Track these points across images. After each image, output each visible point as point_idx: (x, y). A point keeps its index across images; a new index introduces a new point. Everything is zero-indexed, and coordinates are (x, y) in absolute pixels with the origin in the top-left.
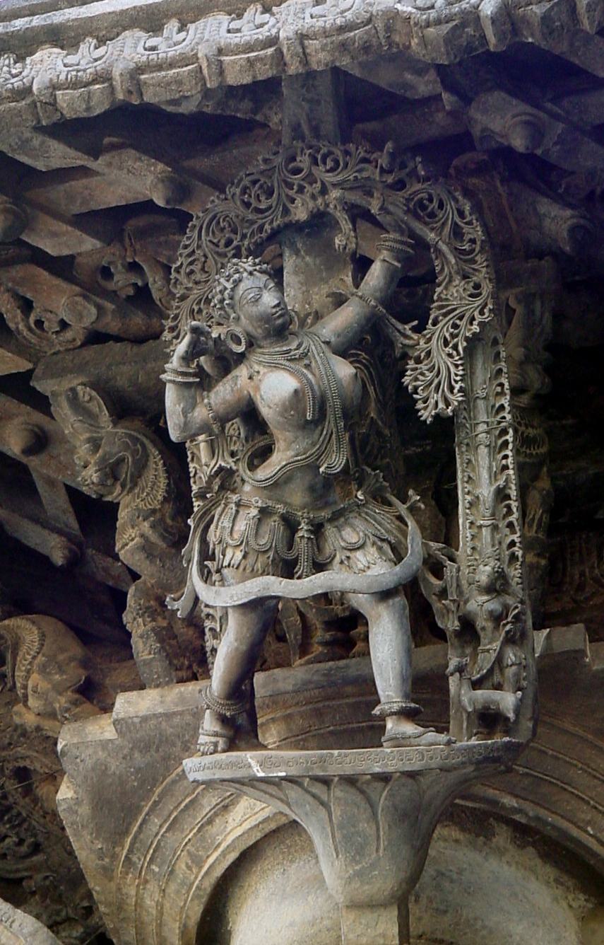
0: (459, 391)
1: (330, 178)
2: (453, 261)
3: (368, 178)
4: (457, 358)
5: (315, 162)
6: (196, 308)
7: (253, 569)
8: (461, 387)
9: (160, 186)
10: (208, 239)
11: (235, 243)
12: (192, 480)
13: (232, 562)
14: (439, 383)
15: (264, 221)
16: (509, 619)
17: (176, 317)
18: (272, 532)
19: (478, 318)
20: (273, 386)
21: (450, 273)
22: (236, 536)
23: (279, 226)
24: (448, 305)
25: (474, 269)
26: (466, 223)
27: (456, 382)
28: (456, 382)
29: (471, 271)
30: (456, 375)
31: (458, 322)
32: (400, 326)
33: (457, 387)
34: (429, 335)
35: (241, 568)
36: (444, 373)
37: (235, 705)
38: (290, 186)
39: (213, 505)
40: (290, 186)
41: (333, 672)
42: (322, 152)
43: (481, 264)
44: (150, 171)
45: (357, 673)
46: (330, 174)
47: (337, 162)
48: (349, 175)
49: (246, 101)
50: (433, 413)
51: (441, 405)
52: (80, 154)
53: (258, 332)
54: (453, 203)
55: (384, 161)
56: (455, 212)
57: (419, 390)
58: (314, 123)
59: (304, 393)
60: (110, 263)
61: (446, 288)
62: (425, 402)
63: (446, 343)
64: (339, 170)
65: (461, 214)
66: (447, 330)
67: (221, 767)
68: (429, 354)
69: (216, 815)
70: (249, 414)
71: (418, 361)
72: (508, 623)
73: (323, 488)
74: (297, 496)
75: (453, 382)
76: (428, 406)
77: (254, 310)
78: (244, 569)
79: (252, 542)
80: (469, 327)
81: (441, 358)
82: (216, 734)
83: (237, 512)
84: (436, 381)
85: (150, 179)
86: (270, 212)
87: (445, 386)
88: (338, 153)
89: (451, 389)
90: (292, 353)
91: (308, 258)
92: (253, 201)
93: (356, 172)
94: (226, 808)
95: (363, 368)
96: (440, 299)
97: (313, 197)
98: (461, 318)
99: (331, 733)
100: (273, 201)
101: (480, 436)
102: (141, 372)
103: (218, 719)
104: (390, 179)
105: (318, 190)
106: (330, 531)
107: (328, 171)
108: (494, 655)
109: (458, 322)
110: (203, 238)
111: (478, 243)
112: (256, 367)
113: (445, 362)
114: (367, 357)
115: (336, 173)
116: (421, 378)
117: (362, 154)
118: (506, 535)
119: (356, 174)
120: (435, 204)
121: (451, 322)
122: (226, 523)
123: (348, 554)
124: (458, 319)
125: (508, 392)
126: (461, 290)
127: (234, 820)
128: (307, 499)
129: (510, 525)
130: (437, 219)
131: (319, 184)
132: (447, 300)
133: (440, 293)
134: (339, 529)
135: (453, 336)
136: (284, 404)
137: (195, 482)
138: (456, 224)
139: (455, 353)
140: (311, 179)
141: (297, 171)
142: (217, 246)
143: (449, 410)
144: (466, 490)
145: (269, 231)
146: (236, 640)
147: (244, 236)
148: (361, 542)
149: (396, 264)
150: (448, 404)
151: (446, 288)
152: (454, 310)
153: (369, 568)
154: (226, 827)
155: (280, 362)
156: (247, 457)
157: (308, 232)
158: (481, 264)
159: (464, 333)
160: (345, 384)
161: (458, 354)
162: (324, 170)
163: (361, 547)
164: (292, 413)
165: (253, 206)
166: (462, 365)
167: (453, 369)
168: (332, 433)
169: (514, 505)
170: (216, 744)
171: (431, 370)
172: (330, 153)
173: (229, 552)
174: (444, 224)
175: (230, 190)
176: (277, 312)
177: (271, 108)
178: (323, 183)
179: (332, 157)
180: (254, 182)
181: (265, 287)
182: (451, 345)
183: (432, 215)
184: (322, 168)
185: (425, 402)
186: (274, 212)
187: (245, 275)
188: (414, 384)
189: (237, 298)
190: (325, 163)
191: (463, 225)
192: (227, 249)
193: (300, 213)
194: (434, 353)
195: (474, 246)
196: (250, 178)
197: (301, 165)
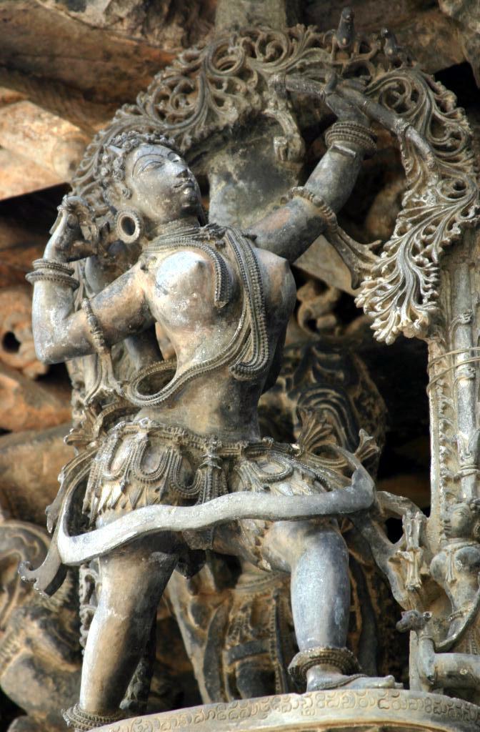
0: (429, 300)
1: (267, 69)
4: (430, 265)
9: (64, 147)
14: (404, 294)
15: (183, 130)
18: (166, 459)
21: (424, 173)
22: (116, 466)
23: (202, 135)
24: (420, 211)
28: (426, 290)
30: (427, 283)
31: (433, 228)
32: (356, 245)
33: (427, 295)
40: (219, 85)
43: (465, 161)
44: (52, 134)
46: (271, 64)
47: (279, 50)
48: (295, 61)
49: (174, 25)
50: (394, 329)
55: (338, 39)
57: (377, 308)
60: (14, 326)
64: (282, 57)
66: (417, 238)
75: (422, 292)
76: (388, 323)
84: (400, 293)
85: (52, 143)
86: (191, 119)
89: (420, 300)
91: (241, 184)
95: (332, 408)
97: (247, 94)
101: (460, 368)
102: (46, 458)
105: (254, 85)
107: (268, 61)
109: (433, 228)
111: (464, 138)
114: (338, 395)
117: (312, 35)
120: (408, 94)
123: (267, 485)
124: (433, 224)
126: (438, 191)
128: (217, 426)
130: (408, 113)
131: (255, 78)
133: (410, 197)
135: (425, 244)
136: (183, 284)
140: (244, 74)
143: (415, 324)
145: (189, 142)
149: (350, 151)
151: (419, 192)
156: (138, 381)
157: (243, 153)
158: (465, 161)
161: (431, 260)
162: (262, 59)
166: (434, 272)
167: (422, 278)
173: (106, 490)
175: (140, 99)
178: (261, 78)
180: (172, 87)
182: (422, 253)
185: (382, 320)
186: (195, 119)
190: (264, 53)
191: (443, 118)
193: (229, 115)
194: (400, 266)
195: (457, 141)
197: (232, 58)
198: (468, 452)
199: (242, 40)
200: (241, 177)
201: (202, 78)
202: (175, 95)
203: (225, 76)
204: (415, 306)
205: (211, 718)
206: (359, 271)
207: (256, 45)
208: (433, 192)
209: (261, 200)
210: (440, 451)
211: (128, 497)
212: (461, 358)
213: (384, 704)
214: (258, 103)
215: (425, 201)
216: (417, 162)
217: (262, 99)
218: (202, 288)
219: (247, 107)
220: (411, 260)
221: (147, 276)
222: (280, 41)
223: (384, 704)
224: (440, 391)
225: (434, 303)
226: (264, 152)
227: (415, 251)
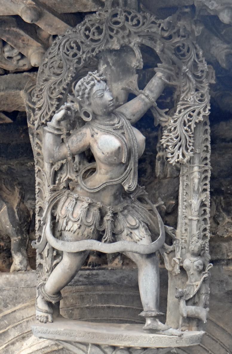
0: (191, 151)
1: (133, 29)
2: (194, 83)
3: (155, 33)
5: (127, 19)
6: (53, 87)
7: (83, 234)
8: (192, 149)
10: (64, 51)
11: (78, 56)
12: (36, 175)
13: (72, 229)
16: (206, 271)
17: (41, 90)
19: (203, 113)
20: (105, 142)
22: (75, 215)
26: (200, 62)
27: (190, 146)
29: (200, 87)
31: (192, 113)
33: (190, 148)
34: (177, 119)
35: (76, 233)
36: (183, 141)
37: (57, 297)
38: (112, 30)
39: (58, 195)
41: (90, 277)
42: (132, 15)
45: (103, 279)
46: (134, 27)
47: (139, 22)
51: (181, 157)
53: (99, 112)
54: (195, 50)
56: (195, 55)
59: (122, 149)
61: (187, 94)
63: (185, 125)
65: (197, 55)
67: (59, 334)
68: (175, 128)
69: (17, 341)
70: (88, 155)
71: (170, 131)
72: (206, 273)
73: (121, 194)
74: (107, 198)
75: (188, 146)
76: (173, 157)
77: (99, 101)
78: (78, 234)
79: (84, 220)
80: (197, 117)
81: (181, 130)
82: (47, 312)
83: (76, 203)
88: (140, 16)
89: (187, 149)
90: (116, 125)
91: (113, 68)
92: (91, 34)
93: (148, 28)
94: (23, 338)
96: (183, 100)
98: (193, 112)
99: (87, 308)
100: (101, 37)
103: (45, 303)
104: (166, 34)
106: (120, 217)
107: (133, 25)
108: (196, 290)
109: (192, 113)
110: (61, 50)
112: (96, 130)
113: (184, 134)
115: (138, 27)
118: (202, 225)
119: (148, 29)
120: (185, 50)
121: (189, 113)
122: (70, 209)
123: (131, 231)
125: (210, 151)
126: (195, 97)
127: (27, 345)
129: (205, 220)
131: (127, 32)
132: (186, 101)
134: (125, 216)
135: (189, 121)
136: (112, 153)
137: (37, 176)
138: (195, 61)
139: (189, 130)
140: (123, 28)
141: (117, 23)
142: (68, 55)
144: (185, 199)
146: (68, 269)
147: (83, 52)
148: (137, 225)
150: (183, 155)
151: (187, 94)
152: (190, 107)
153: (141, 239)
154: (21, 347)
155: (110, 130)
159: (195, 120)
160: (140, 144)
161: (191, 131)
162: (132, 24)
163: (137, 228)
164: (115, 158)
165: (90, 38)
166: (193, 137)
167: (188, 138)
168: (131, 169)
169: (208, 210)
170: (47, 318)
171: (177, 137)
172: (136, 16)
173: (70, 223)
174: (189, 61)
176: (111, 104)
178: (129, 31)
180: (92, 25)
181: (106, 89)
182: (187, 125)
183: (184, 55)
184: (130, 23)
187: (96, 81)
188: (167, 144)
189: (92, 94)
190: (132, 20)
192: (73, 59)
194: (178, 128)
197: (119, 20)
198: (196, 211)
199: (124, 14)
200: (113, 65)
201: (106, 26)
202: (93, 29)
203: (115, 27)
204: (185, 152)
205: (117, 339)
206: (159, 121)
207: (130, 17)
208: (193, 97)
209: (121, 78)
210: (184, 204)
211: (80, 230)
212: (196, 169)
213: (178, 342)
214: (127, 42)
215: (190, 101)
216: (188, 82)
217: (129, 40)
218: (118, 155)
219: (123, 44)
220: (183, 128)
221: (93, 139)
222: (139, 18)
223: (178, 342)
224: (185, 178)
225: (193, 153)
227: (185, 125)
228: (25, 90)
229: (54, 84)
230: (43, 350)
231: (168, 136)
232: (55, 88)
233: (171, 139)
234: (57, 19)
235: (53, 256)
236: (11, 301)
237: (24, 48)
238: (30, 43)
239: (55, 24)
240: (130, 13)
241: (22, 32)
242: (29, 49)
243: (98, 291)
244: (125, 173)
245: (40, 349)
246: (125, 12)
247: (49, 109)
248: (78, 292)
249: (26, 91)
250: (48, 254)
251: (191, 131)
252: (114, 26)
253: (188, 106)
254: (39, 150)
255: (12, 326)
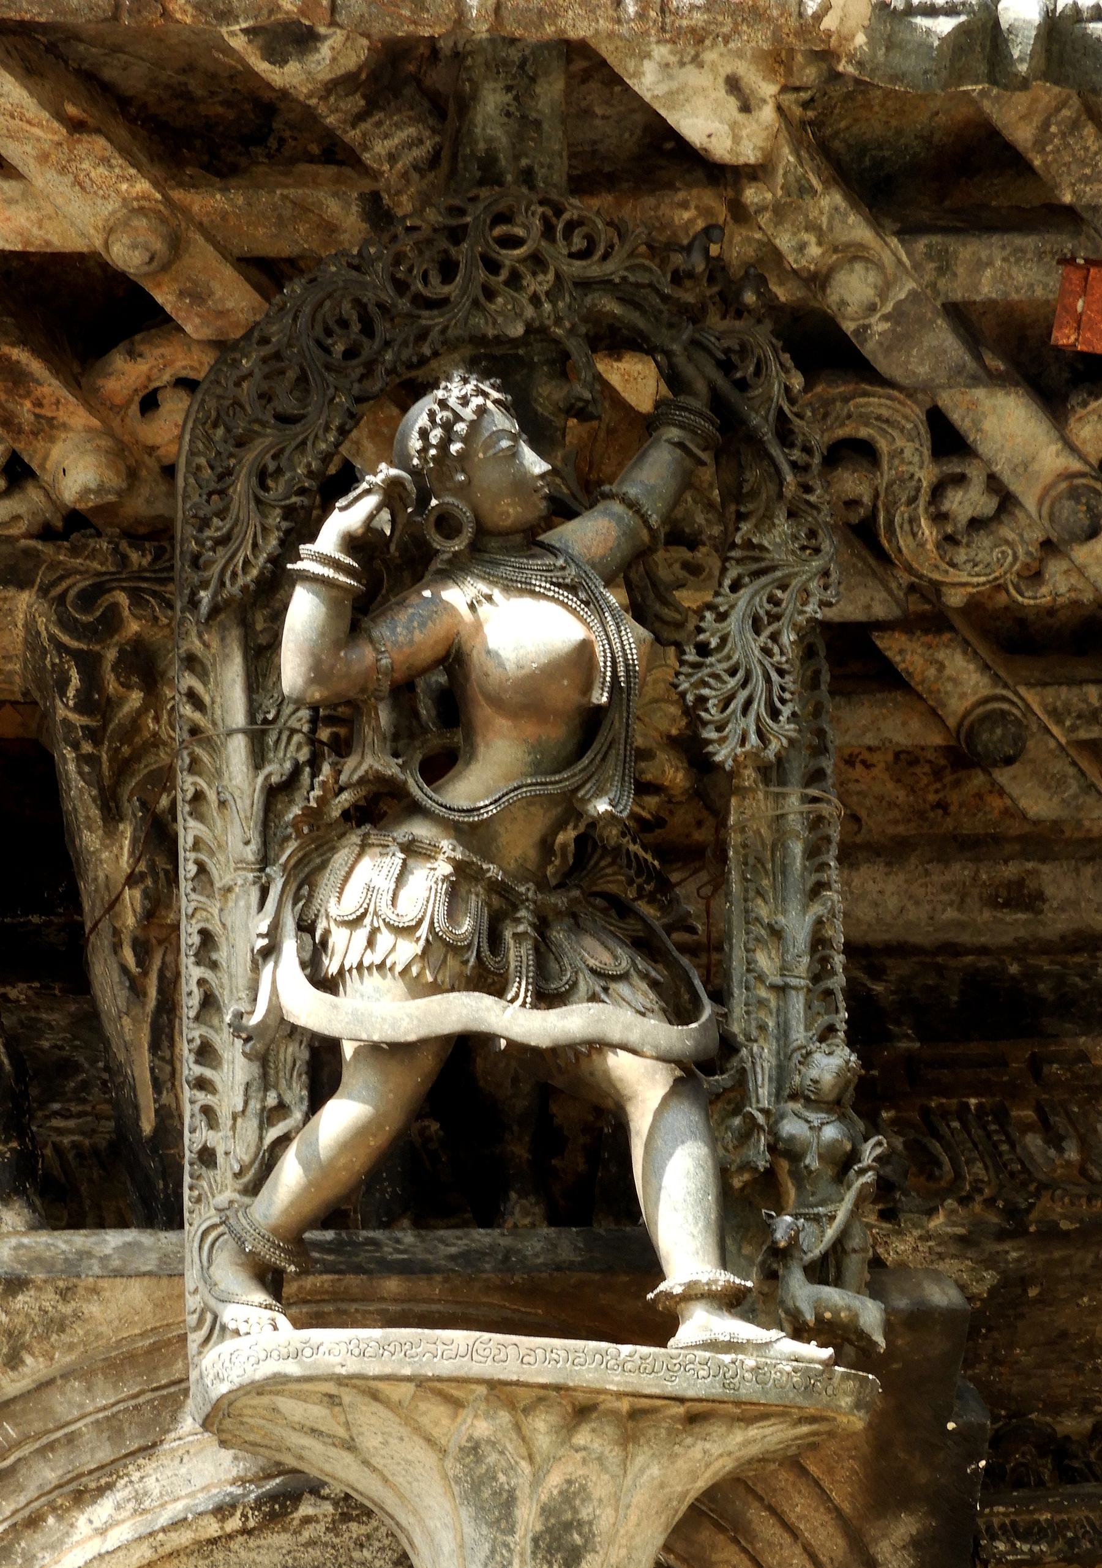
0: (789, 721)
5: (548, 232)
8: (794, 714)
25: (808, 502)
27: (783, 701)
28: (783, 701)
31: (779, 593)
33: (786, 711)
38: (493, 266)
42: (566, 216)
51: (753, 738)
52: (45, 115)
58: (524, 162)
62: (720, 728)
68: (724, 640)
75: (778, 704)
81: (747, 647)
84: (742, 695)
87: (759, 707)
89: (775, 714)
96: (749, 545)
97: (535, 300)
105: (546, 287)
106: (558, 935)
107: (571, 255)
109: (779, 593)
116: (712, 681)
131: (551, 276)
132: (762, 548)
135: (775, 618)
138: (780, 410)
139: (776, 649)
140: (537, 261)
141: (514, 242)
152: (774, 568)
162: (565, 252)
167: (775, 676)
171: (733, 672)
173: (385, 939)
177: (379, 124)
178: (558, 276)
179: (585, 229)
196: (416, 236)
197: (520, 232)
226: (518, 377)
228: (40, 589)
229: (275, 457)
230: (161, 1536)
231: (697, 666)
232: (279, 471)
233: (716, 676)
234: (228, 272)
235: (263, 1109)
236: (41, 1338)
237: (35, 434)
238: (62, 416)
239: (219, 293)
240: (559, 212)
241: (37, 367)
242: (52, 440)
243: (383, 1299)
244: (590, 755)
245: (151, 1534)
246: (541, 203)
247: (255, 545)
248: (305, 1302)
249: (44, 591)
250: (246, 1103)
251: (782, 653)
252: (504, 252)
253: (763, 564)
254: (197, 716)
255: (37, 1445)
